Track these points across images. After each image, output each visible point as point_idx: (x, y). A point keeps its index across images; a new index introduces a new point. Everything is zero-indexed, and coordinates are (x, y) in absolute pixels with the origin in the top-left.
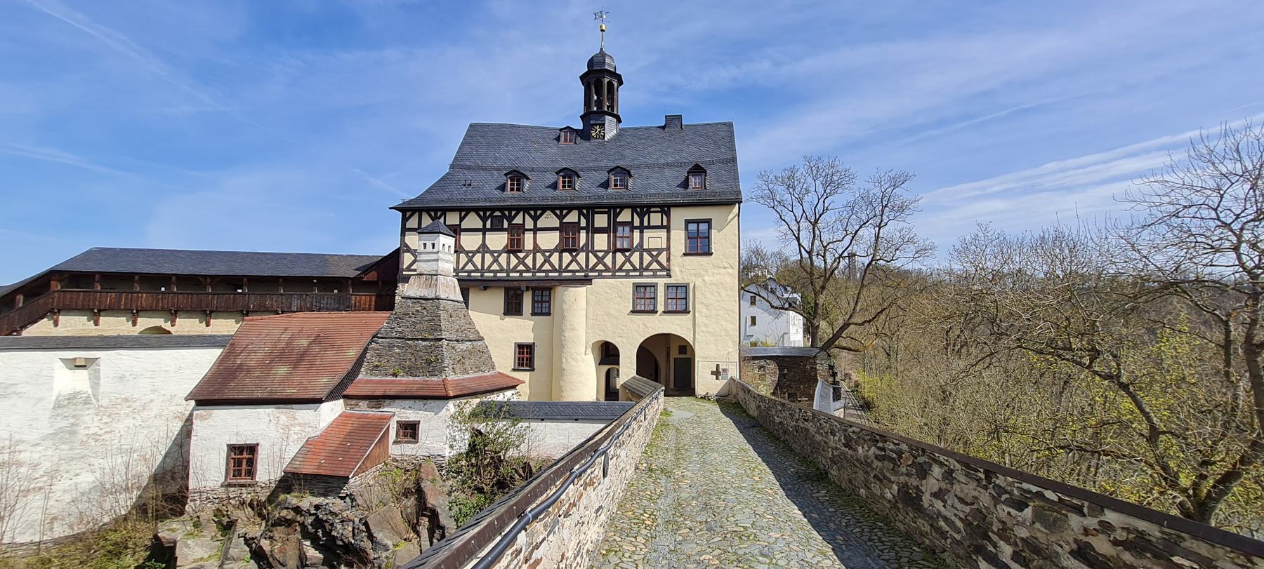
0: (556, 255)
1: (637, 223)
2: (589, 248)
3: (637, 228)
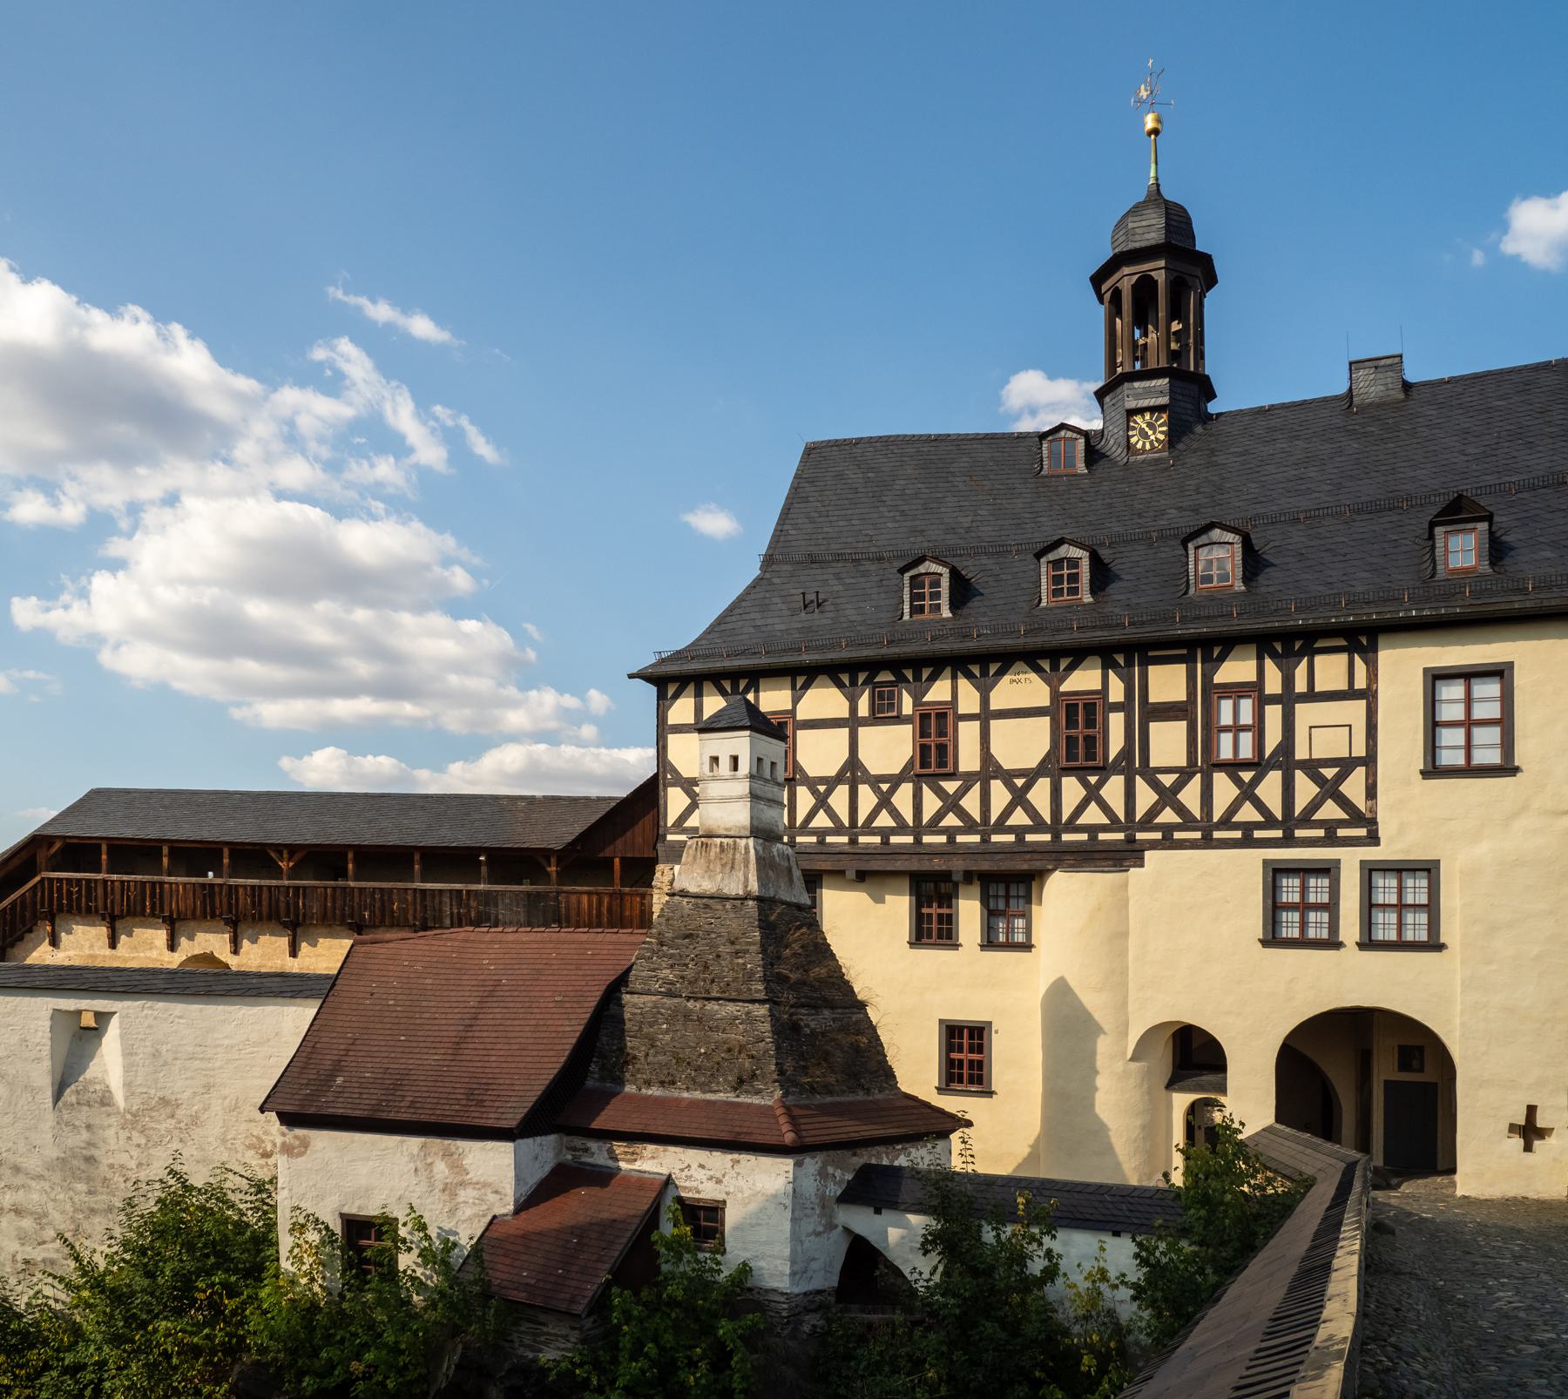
0: (1044, 784)
1: (1273, 684)
2: (1134, 764)
3: (1274, 700)
